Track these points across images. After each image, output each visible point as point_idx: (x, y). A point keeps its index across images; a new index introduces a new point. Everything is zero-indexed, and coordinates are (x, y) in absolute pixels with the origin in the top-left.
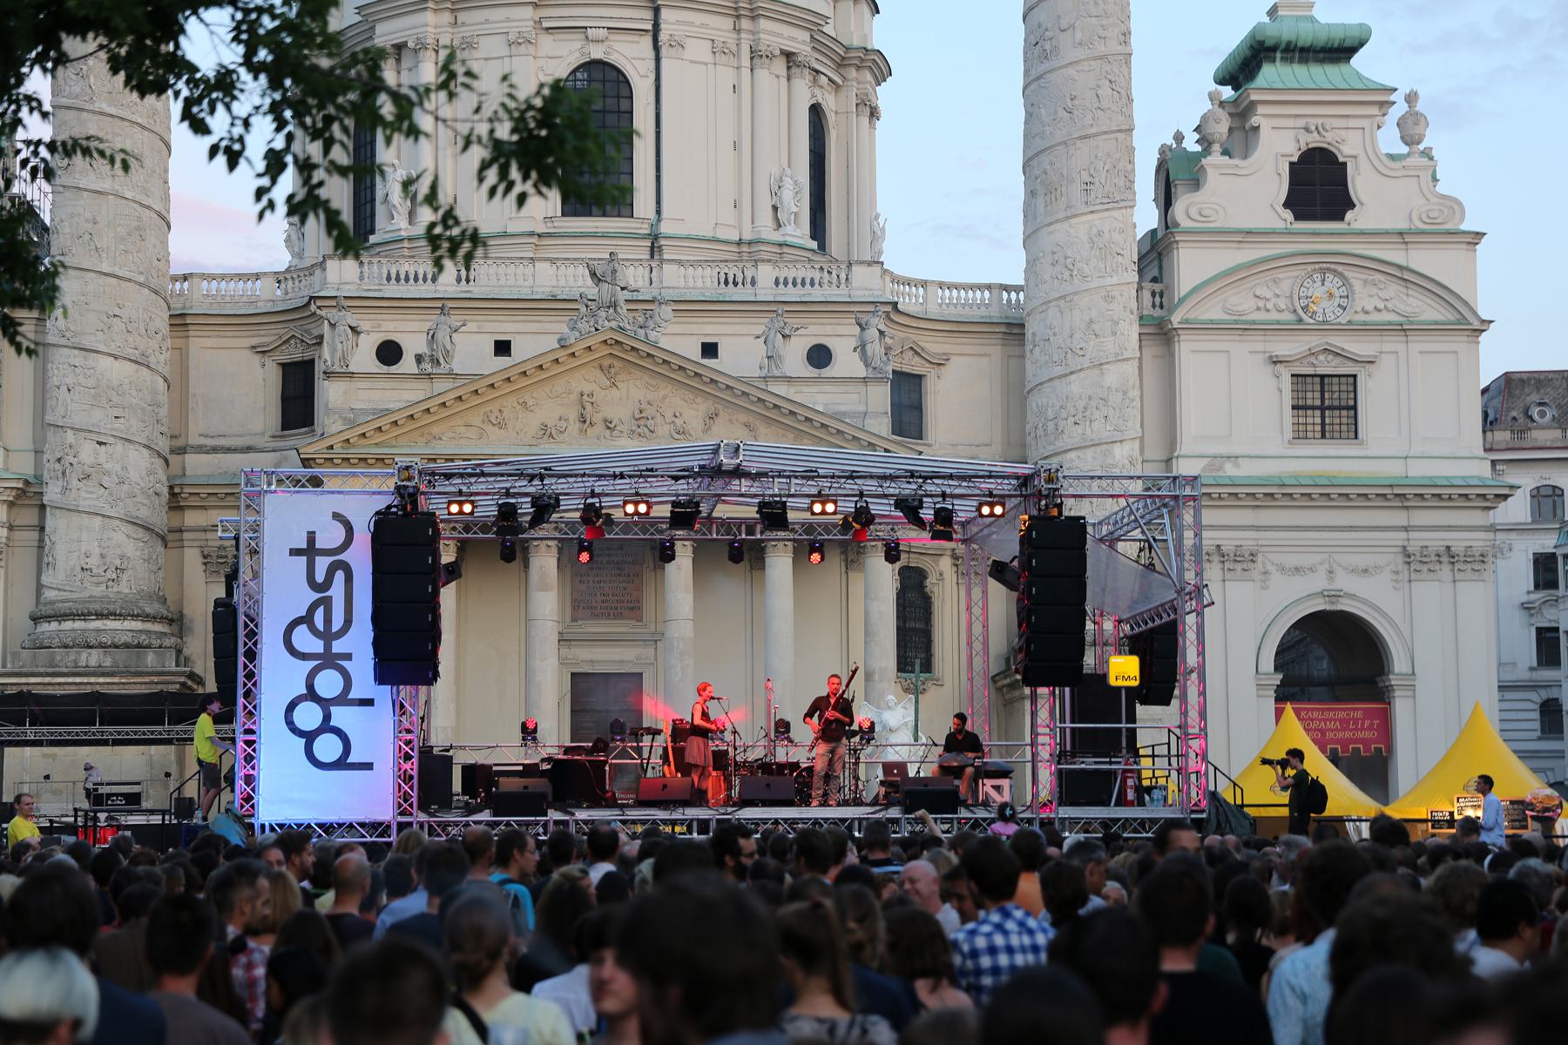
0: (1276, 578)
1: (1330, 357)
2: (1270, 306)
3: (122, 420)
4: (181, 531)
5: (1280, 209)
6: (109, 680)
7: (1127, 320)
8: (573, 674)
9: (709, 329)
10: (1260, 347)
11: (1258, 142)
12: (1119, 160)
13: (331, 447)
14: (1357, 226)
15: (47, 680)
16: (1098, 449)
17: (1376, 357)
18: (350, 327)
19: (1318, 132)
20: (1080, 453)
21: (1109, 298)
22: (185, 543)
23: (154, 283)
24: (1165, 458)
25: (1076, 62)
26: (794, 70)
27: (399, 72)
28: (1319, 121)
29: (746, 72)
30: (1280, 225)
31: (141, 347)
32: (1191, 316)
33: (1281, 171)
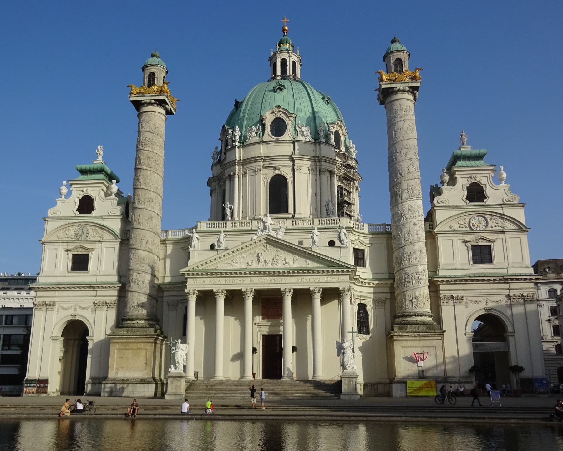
0: (470, 304)
1: (483, 240)
2: (464, 226)
3: (144, 267)
4: (162, 297)
5: (465, 200)
6: (136, 337)
7: (421, 231)
8: (263, 335)
9: (300, 237)
10: (461, 238)
11: (457, 181)
12: (416, 187)
13: (189, 270)
14: (487, 203)
15: (121, 337)
16: (414, 267)
17: (496, 239)
18: (197, 238)
19: (474, 178)
20: (409, 269)
21: (415, 224)
22: (164, 301)
23: (155, 231)
24: (434, 271)
25: (403, 161)
26: (332, 175)
27: (230, 182)
28: (474, 175)
29: (318, 176)
30: (465, 204)
31: (150, 248)
32: (440, 230)
33: (464, 189)
